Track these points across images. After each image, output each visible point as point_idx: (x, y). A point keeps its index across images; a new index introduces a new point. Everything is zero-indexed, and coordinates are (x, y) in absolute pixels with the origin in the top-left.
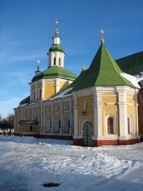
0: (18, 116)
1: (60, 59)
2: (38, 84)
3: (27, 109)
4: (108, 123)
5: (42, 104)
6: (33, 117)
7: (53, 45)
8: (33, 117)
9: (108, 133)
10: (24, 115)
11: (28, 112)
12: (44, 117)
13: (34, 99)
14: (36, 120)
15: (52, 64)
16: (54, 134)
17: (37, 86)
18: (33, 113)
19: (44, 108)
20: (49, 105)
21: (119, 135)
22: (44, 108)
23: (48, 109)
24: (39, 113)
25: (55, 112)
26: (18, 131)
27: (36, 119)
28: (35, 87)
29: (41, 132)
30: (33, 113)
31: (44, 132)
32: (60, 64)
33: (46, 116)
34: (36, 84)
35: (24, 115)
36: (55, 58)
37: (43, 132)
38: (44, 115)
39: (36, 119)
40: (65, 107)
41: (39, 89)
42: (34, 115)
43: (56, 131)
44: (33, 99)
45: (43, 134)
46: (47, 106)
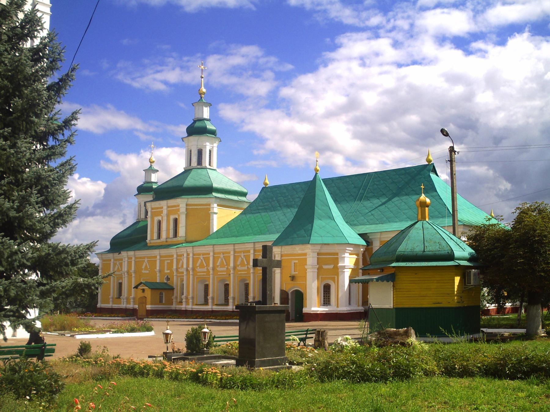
1: (210, 151)
2: (168, 207)
3: (141, 258)
4: (324, 291)
5: (187, 251)
6: (158, 275)
8: (158, 275)
9: (324, 304)
10: (133, 269)
11: (144, 264)
12: (191, 277)
13: (159, 237)
14: (165, 281)
15: (194, 163)
16: (215, 308)
17: (165, 212)
18: (158, 268)
20: (203, 254)
21: (338, 307)
23: (200, 261)
24: (175, 267)
26: (111, 303)
27: (168, 279)
28: (162, 212)
29: (184, 303)
31: (190, 303)
33: (193, 275)
34: (165, 207)
35: (133, 269)
37: (187, 303)
38: (191, 273)
39: (168, 279)
41: (172, 218)
45: (190, 307)
46: (199, 254)
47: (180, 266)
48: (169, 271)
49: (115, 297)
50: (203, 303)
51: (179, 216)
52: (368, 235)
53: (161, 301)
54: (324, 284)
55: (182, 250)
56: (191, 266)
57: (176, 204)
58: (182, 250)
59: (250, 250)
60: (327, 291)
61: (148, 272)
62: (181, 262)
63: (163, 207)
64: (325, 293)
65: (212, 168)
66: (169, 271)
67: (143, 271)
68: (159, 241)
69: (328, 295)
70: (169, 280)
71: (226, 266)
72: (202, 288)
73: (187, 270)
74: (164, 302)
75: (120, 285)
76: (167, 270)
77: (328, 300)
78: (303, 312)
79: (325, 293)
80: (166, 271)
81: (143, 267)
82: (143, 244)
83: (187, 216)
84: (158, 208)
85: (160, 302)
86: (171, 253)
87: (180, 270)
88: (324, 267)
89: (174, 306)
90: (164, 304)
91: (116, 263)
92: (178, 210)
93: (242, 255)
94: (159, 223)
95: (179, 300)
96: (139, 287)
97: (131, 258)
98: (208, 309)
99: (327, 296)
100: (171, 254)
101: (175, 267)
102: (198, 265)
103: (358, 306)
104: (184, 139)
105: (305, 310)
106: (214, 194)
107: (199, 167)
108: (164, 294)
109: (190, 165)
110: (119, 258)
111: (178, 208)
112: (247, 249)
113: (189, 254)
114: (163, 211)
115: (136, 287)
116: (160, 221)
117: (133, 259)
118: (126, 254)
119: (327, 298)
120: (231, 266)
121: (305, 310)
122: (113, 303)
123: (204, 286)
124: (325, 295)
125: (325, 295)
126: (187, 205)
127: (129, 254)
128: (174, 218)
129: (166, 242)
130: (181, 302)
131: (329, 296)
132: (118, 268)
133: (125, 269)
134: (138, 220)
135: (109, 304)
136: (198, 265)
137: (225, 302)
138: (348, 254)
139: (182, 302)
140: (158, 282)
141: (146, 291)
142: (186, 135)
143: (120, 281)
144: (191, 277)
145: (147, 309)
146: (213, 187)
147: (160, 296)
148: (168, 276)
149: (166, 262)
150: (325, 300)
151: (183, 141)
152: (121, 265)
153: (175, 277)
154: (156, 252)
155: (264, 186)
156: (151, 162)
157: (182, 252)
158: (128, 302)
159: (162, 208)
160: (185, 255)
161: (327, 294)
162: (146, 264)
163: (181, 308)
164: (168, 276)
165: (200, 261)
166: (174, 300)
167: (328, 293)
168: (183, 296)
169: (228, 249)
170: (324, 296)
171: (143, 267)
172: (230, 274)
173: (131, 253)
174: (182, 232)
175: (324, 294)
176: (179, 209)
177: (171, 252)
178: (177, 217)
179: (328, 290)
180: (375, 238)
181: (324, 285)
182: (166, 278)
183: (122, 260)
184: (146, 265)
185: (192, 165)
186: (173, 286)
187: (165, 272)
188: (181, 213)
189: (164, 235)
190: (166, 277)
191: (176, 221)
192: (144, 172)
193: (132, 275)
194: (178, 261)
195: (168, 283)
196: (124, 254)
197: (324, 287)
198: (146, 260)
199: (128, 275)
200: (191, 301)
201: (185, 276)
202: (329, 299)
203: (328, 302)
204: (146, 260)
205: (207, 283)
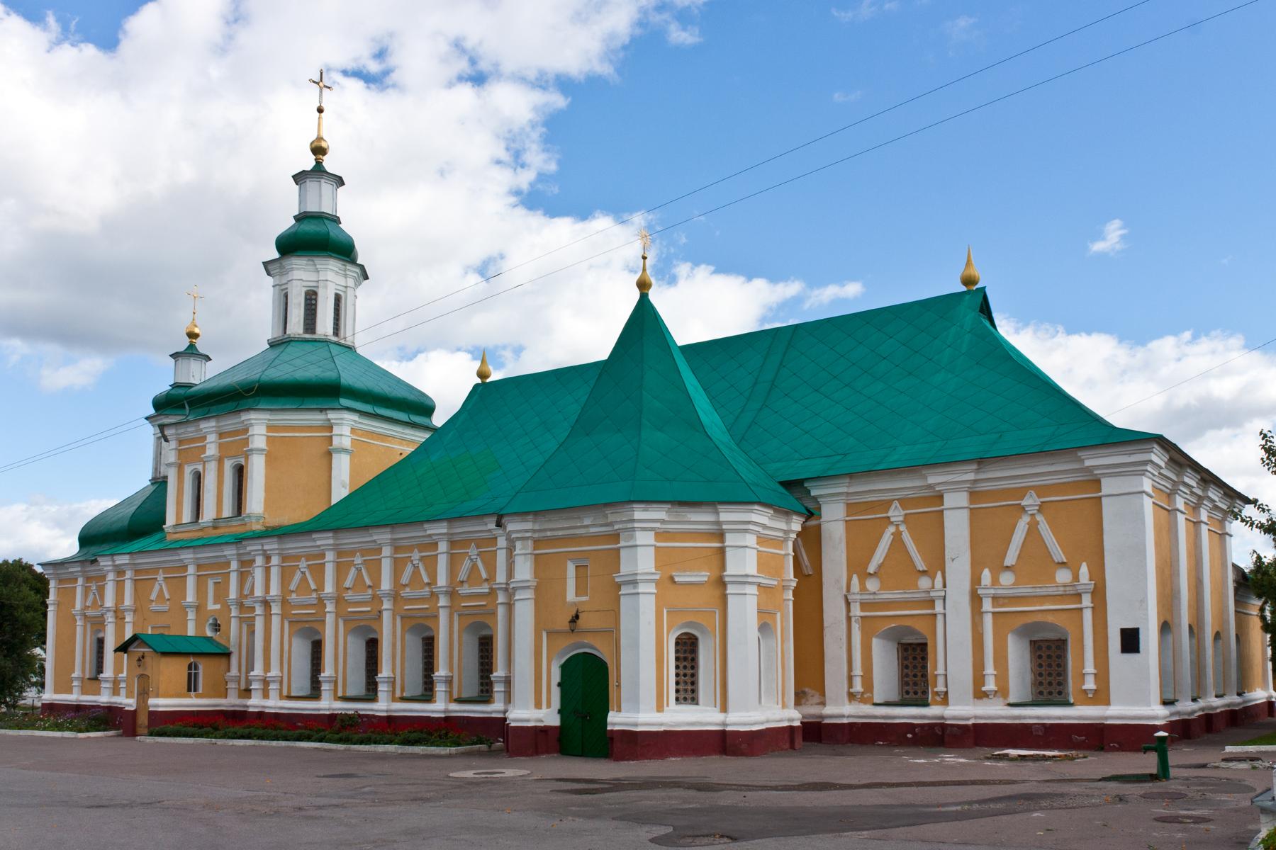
0: (78, 606)
1: (338, 299)
3: (147, 571)
4: (677, 659)
6: (191, 615)
7: (299, 219)
8: (191, 615)
9: (677, 699)
11: (157, 587)
12: (276, 621)
14: (209, 633)
15: (296, 326)
16: (340, 707)
17: (212, 450)
18: (190, 598)
19: (275, 573)
21: (724, 709)
22: (275, 573)
24: (233, 595)
25: (349, 596)
26: (75, 690)
27: (216, 627)
30: (190, 598)
31: (273, 694)
32: (336, 331)
34: (212, 438)
36: (315, 293)
37: (266, 695)
38: (276, 609)
40: (409, 570)
41: (228, 465)
42: (199, 608)
43: (349, 693)
44: (187, 517)
46: (297, 558)
47: (246, 592)
48: (218, 607)
49: (87, 676)
50: (306, 692)
51: (247, 458)
52: (805, 485)
53: (192, 686)
54: (676, 637)
55: (249, 548)
56: (275, 590)
57: (238, 427)
58: (249, 548)
59: (437, 543)
60: (685, 659)
61: (165, 607)
62: (249, 580)
63: (206, 437)
64: (681, 666)
65: (342, 341)
66: (218, 607)
67: (154, 607)
68: (196, 527)
69: (689, 672)
70: (219, 630)
71: (370, 592)
72: (301, 651)
73: (266, 604)
74: (200, 691)
75: (101, 642)
76: (215, 603)
77: (690, 687)
78: (609, 728)
79: (681, 666)
80: (212, 606)
81: (153, 597)
82: (158, 536)
83: (271, 459)
84: (193, 440)
85: (189, 690)
86: (225, 556)
87: (247, 602)
88: (677, 579)
89: (230, 702)
90: (198, 696)
91: (90, 586)
92: (246, 442)
93: (416, 555)
94: (198, 478)
95: (243, 687)
96: (131, 649)
97: (124, 572)
98: (319, 710)
99: (685, 675)
100: (223, 560)
101: (233, 595)
102: (292, 587)
103: (784, 706)
104: (270, 267)
105: (617, 720)
106: (344, 402)
107: (307, 336)
108: (201, 667)
109: (285, 333)
110: (99, 573)
111: (244, 437)
112: (427, 541)
113: (270, 557)
114: (208, 446)
115: (123, 648)
116: (200, 474)
117: (127, 576)
118: (110, 563)
119: (686, 683)
120: (383, 588)
121: (617, 720)
122: (84, 692)
123: (310, 647)
124: (682, 672)
125: (682, 672)
126: (270, 428)
127: (117, 562)
128: (235, 465)
129: (215, 528)
130: (247, 692)
131: (693, 675)
132: (95, 601)
133: (109, 602)
134: (153, 482)
135: (70, 691)
136: (292, 587)
137: (368, 690)
138: (754, 537)
139: (250, 690)
140: (189, 635)
141: (147, 659)
142: (276, 255)
143: (101, 635)
144: (276, 621)
145: (150, 709)
146: (340, 383)
147: (190, 675)
148: (216, 620)
149: (211, 583)
150: (681, 687)
151: (269, 274)
152: (101, 590)
153: (234, 623)
154: (187, 556)
155: (480, 382)
156: (193, 335)
157: (249, 553)
158: (116, 691)
159: (204, 438)
160: (259, 561)
161: (685, 667)
162: (161, 590)
163: (248, 707)
164: (216, 620)
165: (298, 576)
166: (231, 685)
167: (689, 666)
168: (252, 673)
169: (375, 541)
170: (677, 675)
171: (153, 597)
172: (380, 612)
173: (122, 560)
174: (256, 502)
175: (677, 667)
176: (248, 439)
177: (225, 553)
178: (243, 464)
179: (690, 657)
180: (821, 496)
181: (676, 639)
182: (210, 624)
183: (103, 578)
184: (161, 590)
185: (288, 332)
186: (227, 645)
187: (209, 608)
188: (252, 450)
189: (208, 514)
190: (211, 621)
191: (240, 472)
192: (172, 361)
193: (124, 618)
194: (243, 576)
195: (218, 639)
196: (105, 563)
197: (677, 644)
198: (160, 577)
199: (116, 618)
200: (272, 686)
201: (257, 618)
202: (693, 683)
203: (689, 695)
204: (160, 577)
205: (317, 638)
